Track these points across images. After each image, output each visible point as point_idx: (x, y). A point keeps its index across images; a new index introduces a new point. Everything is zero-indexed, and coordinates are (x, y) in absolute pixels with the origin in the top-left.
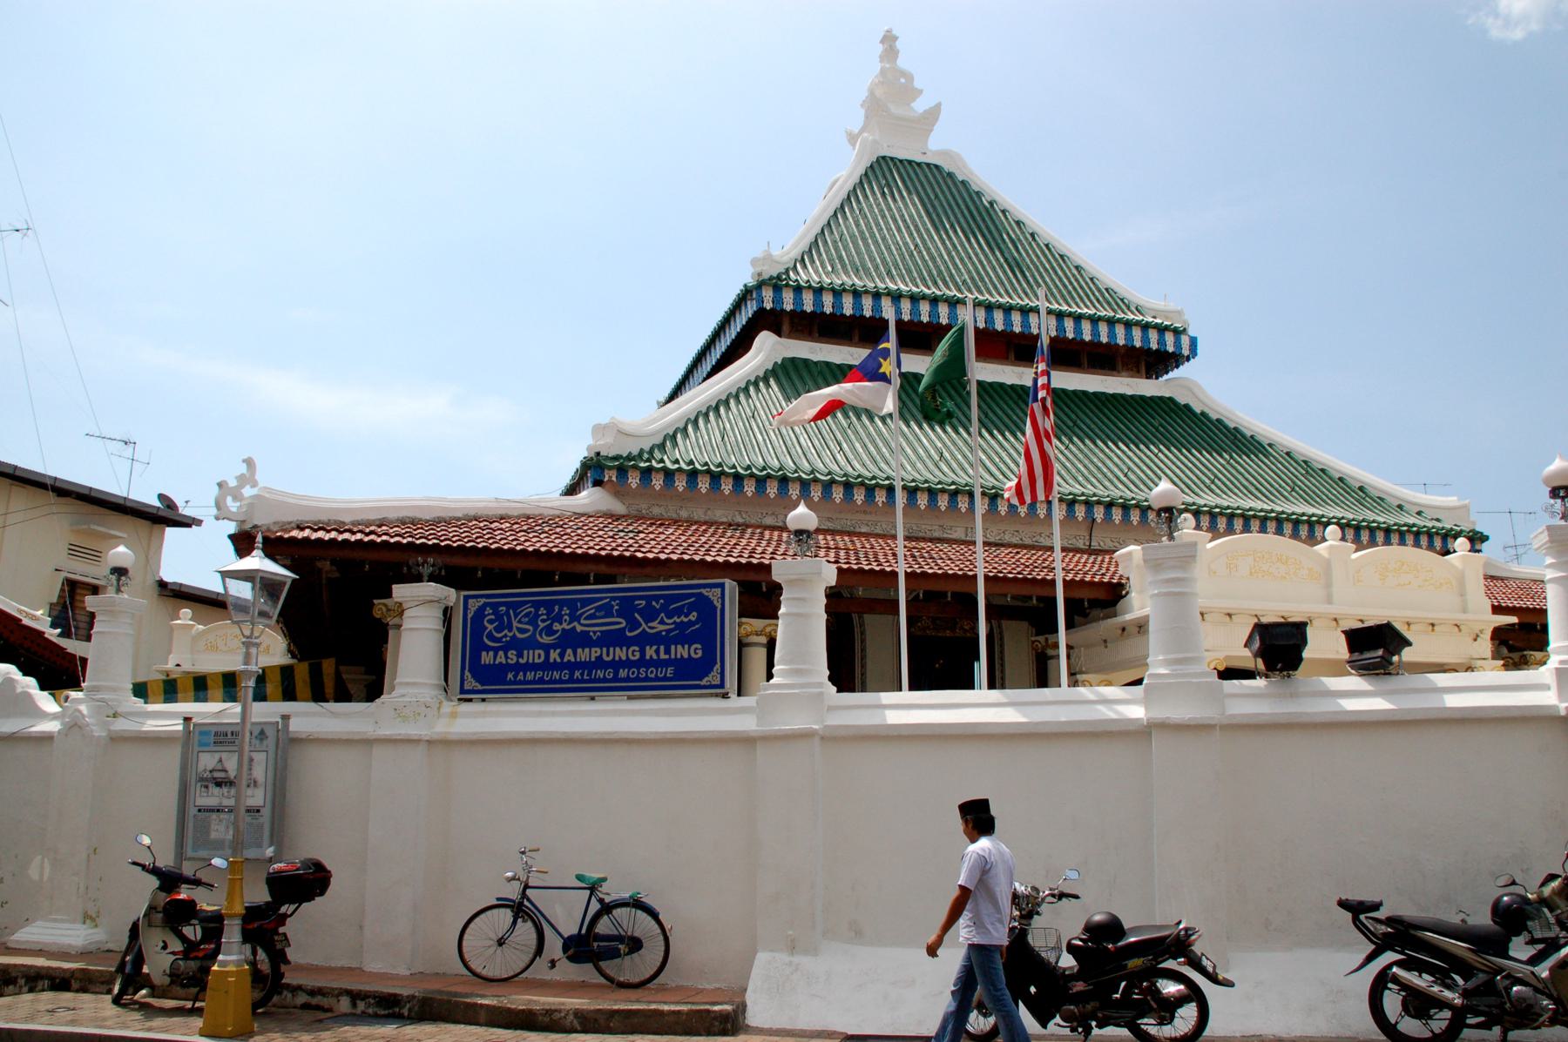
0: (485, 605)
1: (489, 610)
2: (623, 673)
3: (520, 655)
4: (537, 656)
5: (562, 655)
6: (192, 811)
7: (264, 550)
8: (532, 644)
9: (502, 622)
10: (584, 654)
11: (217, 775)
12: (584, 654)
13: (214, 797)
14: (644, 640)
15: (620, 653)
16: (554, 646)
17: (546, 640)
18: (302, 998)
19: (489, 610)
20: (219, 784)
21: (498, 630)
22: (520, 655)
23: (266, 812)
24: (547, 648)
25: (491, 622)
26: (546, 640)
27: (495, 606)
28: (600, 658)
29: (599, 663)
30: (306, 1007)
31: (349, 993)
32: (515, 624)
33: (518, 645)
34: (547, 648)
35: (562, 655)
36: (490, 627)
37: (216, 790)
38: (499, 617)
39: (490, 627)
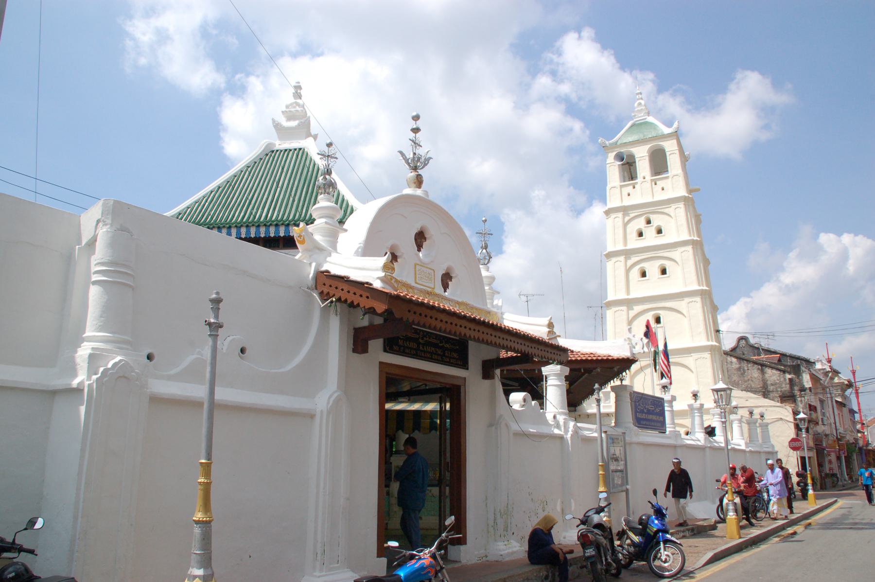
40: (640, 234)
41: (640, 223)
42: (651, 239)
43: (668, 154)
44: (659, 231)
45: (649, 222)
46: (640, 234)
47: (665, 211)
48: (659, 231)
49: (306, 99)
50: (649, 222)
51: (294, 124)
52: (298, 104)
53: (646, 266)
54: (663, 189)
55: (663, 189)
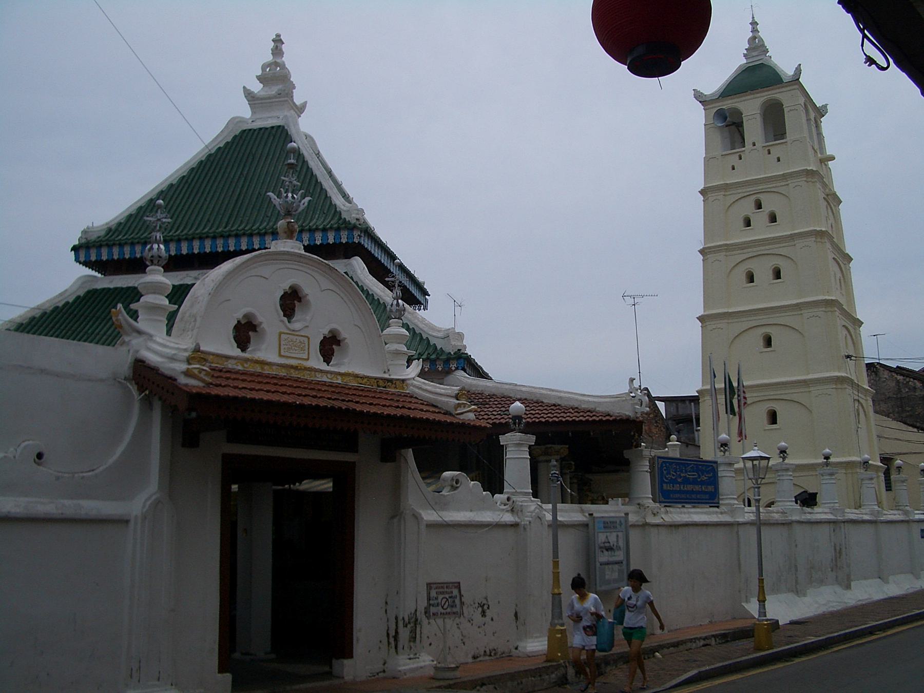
6: (598, 565)
10: (689, 487)
11: (607, 545)
12: (689, 487)
13: (603, 557)
14: (702, 483)
15: (697, 488)
18: (702, 642)
20: (607, 550)
23: (624, 562)
29: (692, 492)
30: (704, 645)
31: (713, 636)
33: (673, 482)
34: (680, 483)
37: (606, 553)
40: (748, 223)
41: (747, 207)
42: (761, 230)
43: (786, 110)
44: (773, 218)
45: (759, 206)
46: (748, 223)
47: (780, 190)
48: (773, 218)
49: (288, 59)
50: (759, 206)
51: (273, 90)
52: (276, 64)
53: (753, 265)
54: (779, 160)
55: (779, 160)
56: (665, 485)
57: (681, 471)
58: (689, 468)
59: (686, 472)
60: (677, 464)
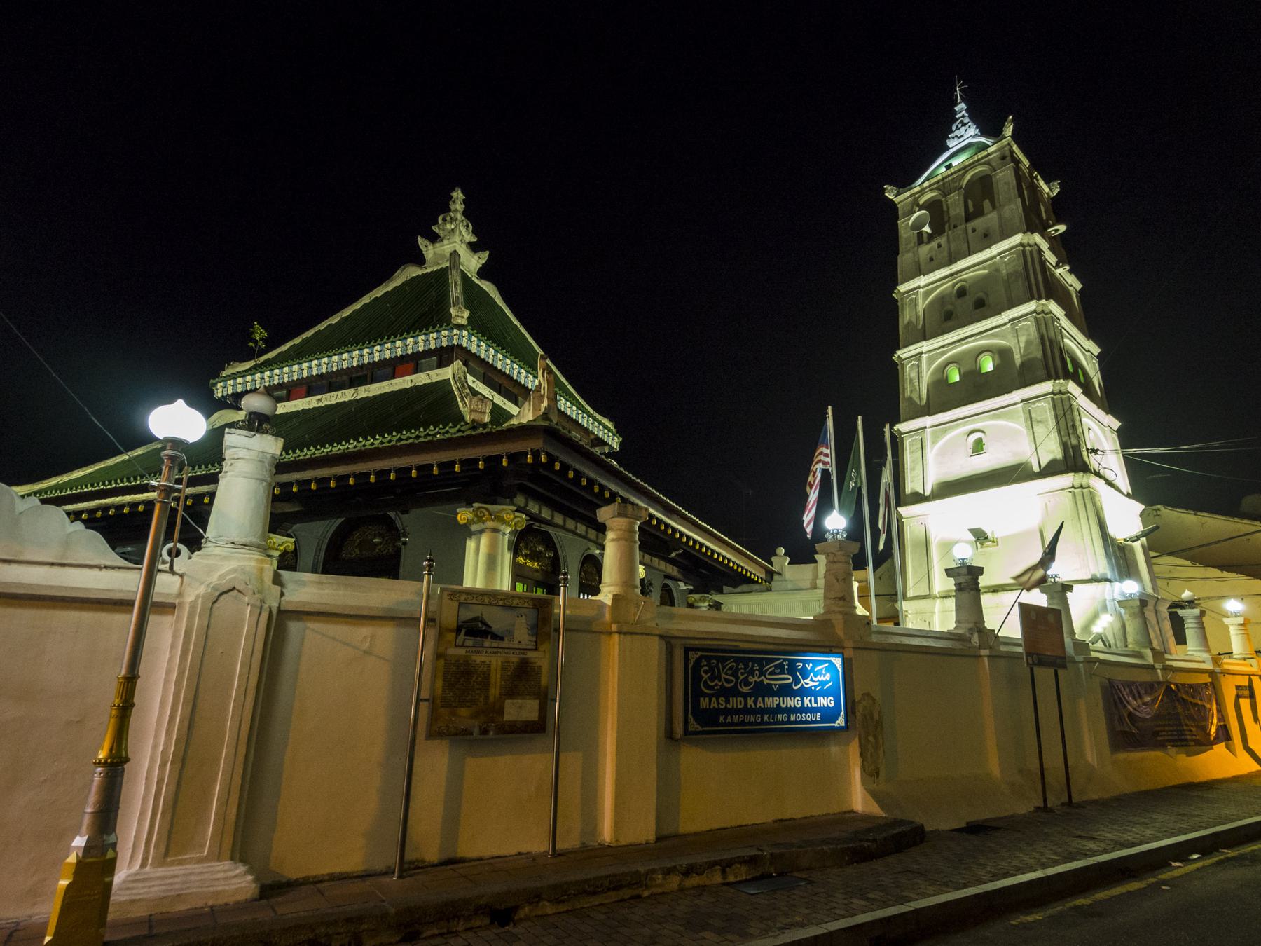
0: (702, 657)
1: (704, 662)
2: (793, 717)
3: (727, 702)
4: (738, 703)
5: (755, 702)
7: (1068, 292)
8: (734, 692)
9: (713, 673)
16: (750, 695)
17: (745, 689)
19: (704, 662)
21: (712, 679)
22: (727, 702)
24: (745, 696)
25: (706, 672)
26: (745, 689)
27: (708, 659)
28: (779, 705)
32: (723, 675)
34: (745, 696)
35: (755, 702)
36: (706, 677)
38: (711, 669)
39: (706, 677)
56: (704, 703)
57: (752, 673)
58: (771, 667)
59: (762, 673)
60: (737, 660)
